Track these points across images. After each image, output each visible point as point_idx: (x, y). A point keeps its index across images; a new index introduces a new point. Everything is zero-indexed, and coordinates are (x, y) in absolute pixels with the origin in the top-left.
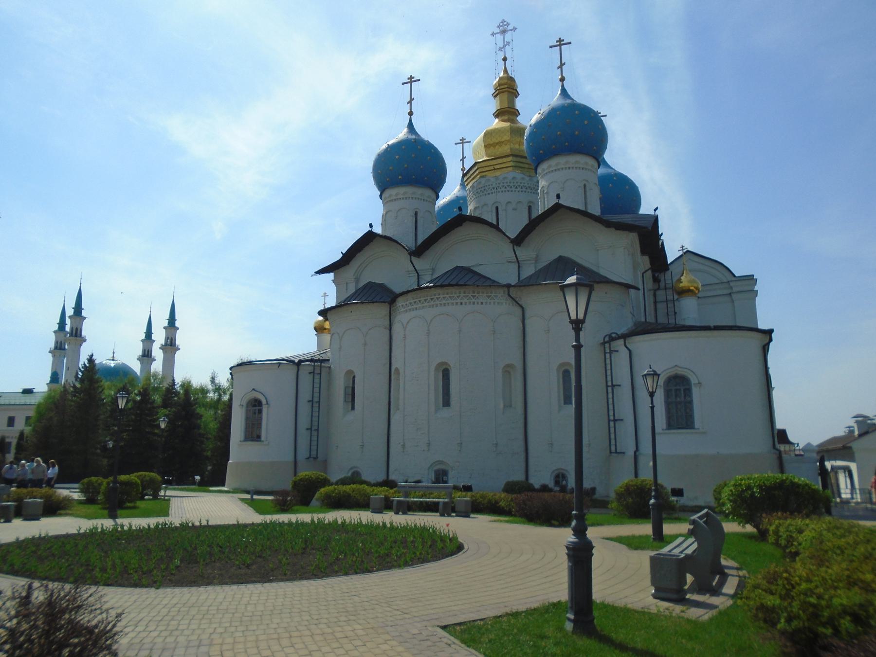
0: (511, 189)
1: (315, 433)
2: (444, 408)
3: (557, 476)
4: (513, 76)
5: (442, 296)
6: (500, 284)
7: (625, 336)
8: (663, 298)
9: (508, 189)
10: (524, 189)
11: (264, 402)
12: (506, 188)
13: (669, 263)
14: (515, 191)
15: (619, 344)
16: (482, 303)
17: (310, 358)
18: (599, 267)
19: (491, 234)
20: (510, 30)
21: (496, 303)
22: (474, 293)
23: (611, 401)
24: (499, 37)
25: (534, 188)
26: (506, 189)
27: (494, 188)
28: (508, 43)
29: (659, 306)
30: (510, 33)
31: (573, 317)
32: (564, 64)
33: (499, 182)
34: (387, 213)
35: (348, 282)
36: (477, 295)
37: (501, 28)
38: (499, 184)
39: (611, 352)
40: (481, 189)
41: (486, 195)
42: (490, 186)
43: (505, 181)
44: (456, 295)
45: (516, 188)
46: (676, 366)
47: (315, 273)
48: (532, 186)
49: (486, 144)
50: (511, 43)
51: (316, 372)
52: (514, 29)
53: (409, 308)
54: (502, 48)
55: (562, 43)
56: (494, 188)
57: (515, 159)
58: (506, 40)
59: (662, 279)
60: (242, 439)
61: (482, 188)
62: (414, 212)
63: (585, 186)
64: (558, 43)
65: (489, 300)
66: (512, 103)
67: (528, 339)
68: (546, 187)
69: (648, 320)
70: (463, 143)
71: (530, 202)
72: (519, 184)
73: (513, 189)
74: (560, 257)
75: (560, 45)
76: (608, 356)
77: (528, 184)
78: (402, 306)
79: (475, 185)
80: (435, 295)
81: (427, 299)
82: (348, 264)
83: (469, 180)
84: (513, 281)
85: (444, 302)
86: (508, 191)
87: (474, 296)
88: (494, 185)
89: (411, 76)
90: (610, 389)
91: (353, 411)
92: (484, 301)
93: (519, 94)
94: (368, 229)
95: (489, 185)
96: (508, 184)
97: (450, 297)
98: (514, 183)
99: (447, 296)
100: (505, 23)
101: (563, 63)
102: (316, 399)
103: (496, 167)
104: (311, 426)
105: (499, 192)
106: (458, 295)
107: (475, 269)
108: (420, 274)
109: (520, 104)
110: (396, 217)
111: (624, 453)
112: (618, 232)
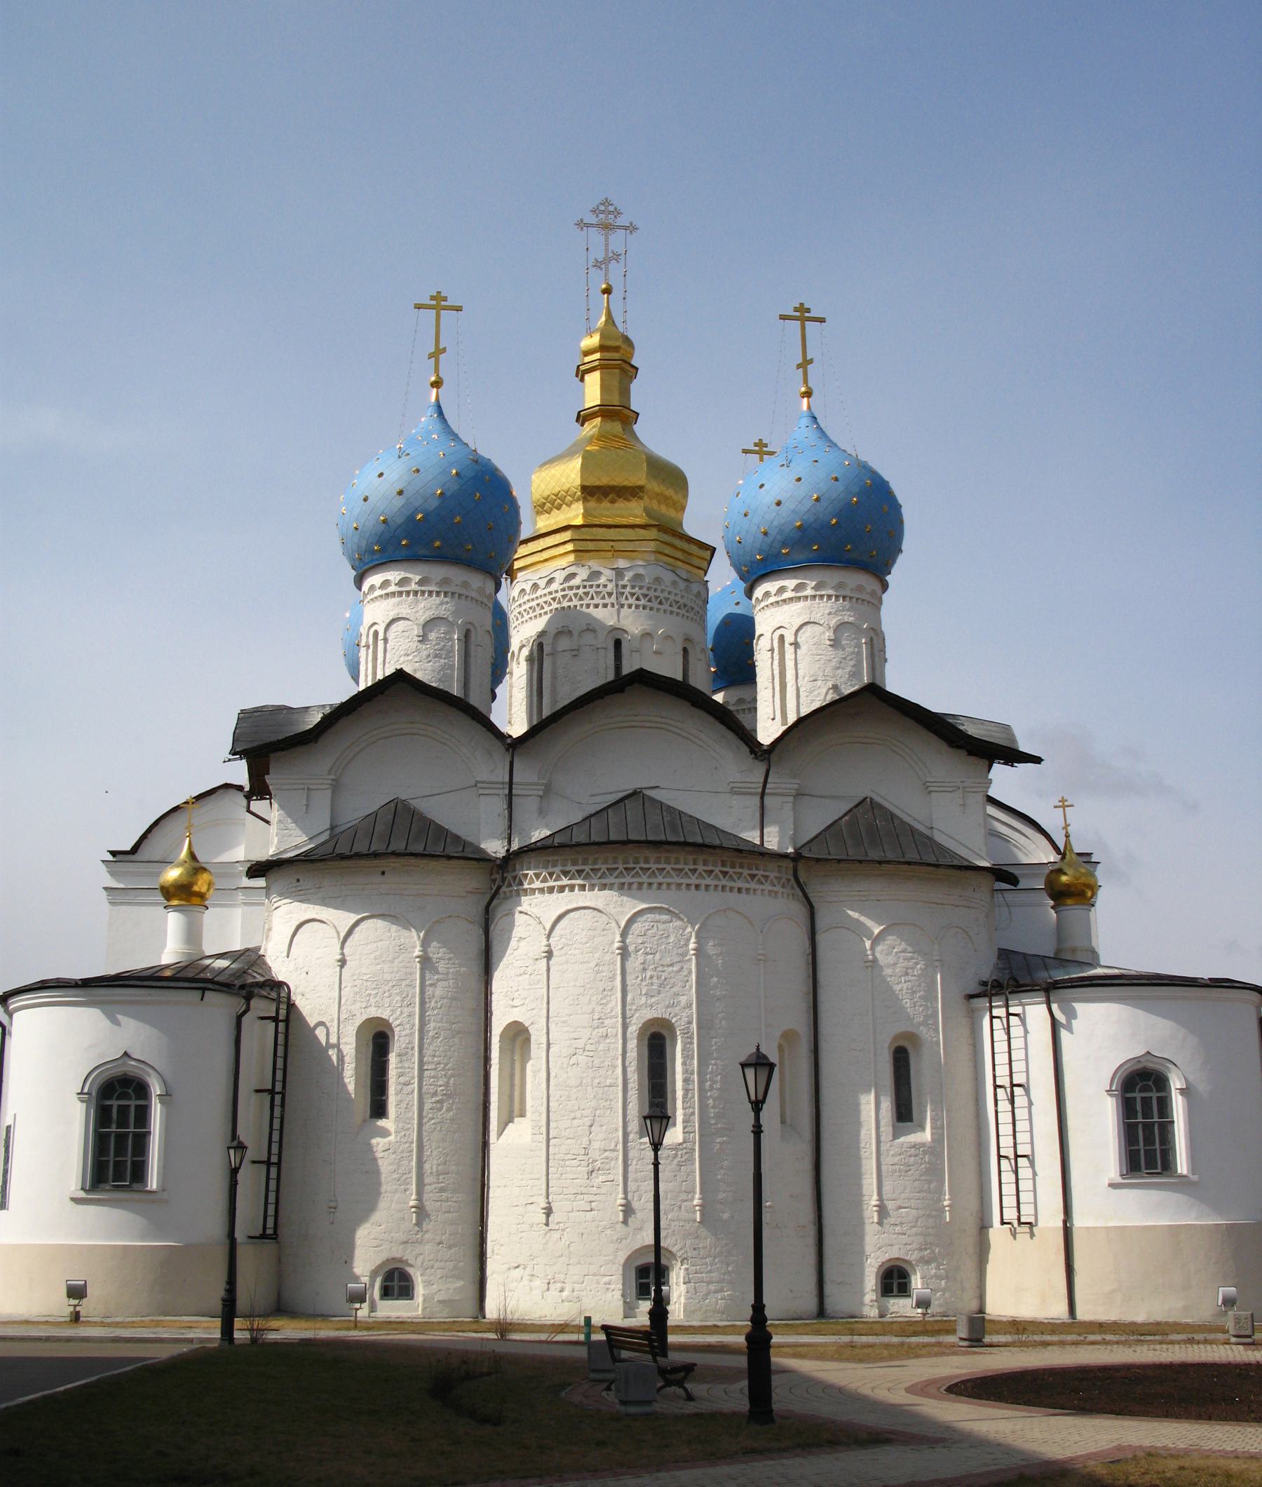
5: (654, 867)
10: (675, 609)
11: (156, 1089)
16: (739, 890)
18: (932, 828)
20: (626, 228)
21: (766, 892)
22: (724, 864)
24: (596, 236)
27: (610, 594)
28: (617, 257)
35: (311, 787)
37: (601, 216)
38: (624, 587)
40: (574, 591)
42: (601, 588)
44: (687, 868)
45: (660, 603)
48: (689, 604)
49: (586, 484)
50: (622, 257)
52: (631, 228)
53: (559, 883)
55: (807, 315)
56: (610, 594)
58: (610, 248)
61: (578, 587)
63: (872, 640)
65: (753, 885)
66: (625, 392)
72: (666, 595)
73: (655, 604)
77: (682, 597)
79: (560, 576)
81: (618, 868)
82: (316, 742)
85: (660, 879)
87: (725, 874)
88: (610, 587)
92: (744, 885)
96: (644, 591)
97: (672, 869)
98: (655, 590)
99: (668, 867)
103: (619, 546)
104: (269, 1158)
106: (692, 867)
110: (423, 639)
112: (972, 758)
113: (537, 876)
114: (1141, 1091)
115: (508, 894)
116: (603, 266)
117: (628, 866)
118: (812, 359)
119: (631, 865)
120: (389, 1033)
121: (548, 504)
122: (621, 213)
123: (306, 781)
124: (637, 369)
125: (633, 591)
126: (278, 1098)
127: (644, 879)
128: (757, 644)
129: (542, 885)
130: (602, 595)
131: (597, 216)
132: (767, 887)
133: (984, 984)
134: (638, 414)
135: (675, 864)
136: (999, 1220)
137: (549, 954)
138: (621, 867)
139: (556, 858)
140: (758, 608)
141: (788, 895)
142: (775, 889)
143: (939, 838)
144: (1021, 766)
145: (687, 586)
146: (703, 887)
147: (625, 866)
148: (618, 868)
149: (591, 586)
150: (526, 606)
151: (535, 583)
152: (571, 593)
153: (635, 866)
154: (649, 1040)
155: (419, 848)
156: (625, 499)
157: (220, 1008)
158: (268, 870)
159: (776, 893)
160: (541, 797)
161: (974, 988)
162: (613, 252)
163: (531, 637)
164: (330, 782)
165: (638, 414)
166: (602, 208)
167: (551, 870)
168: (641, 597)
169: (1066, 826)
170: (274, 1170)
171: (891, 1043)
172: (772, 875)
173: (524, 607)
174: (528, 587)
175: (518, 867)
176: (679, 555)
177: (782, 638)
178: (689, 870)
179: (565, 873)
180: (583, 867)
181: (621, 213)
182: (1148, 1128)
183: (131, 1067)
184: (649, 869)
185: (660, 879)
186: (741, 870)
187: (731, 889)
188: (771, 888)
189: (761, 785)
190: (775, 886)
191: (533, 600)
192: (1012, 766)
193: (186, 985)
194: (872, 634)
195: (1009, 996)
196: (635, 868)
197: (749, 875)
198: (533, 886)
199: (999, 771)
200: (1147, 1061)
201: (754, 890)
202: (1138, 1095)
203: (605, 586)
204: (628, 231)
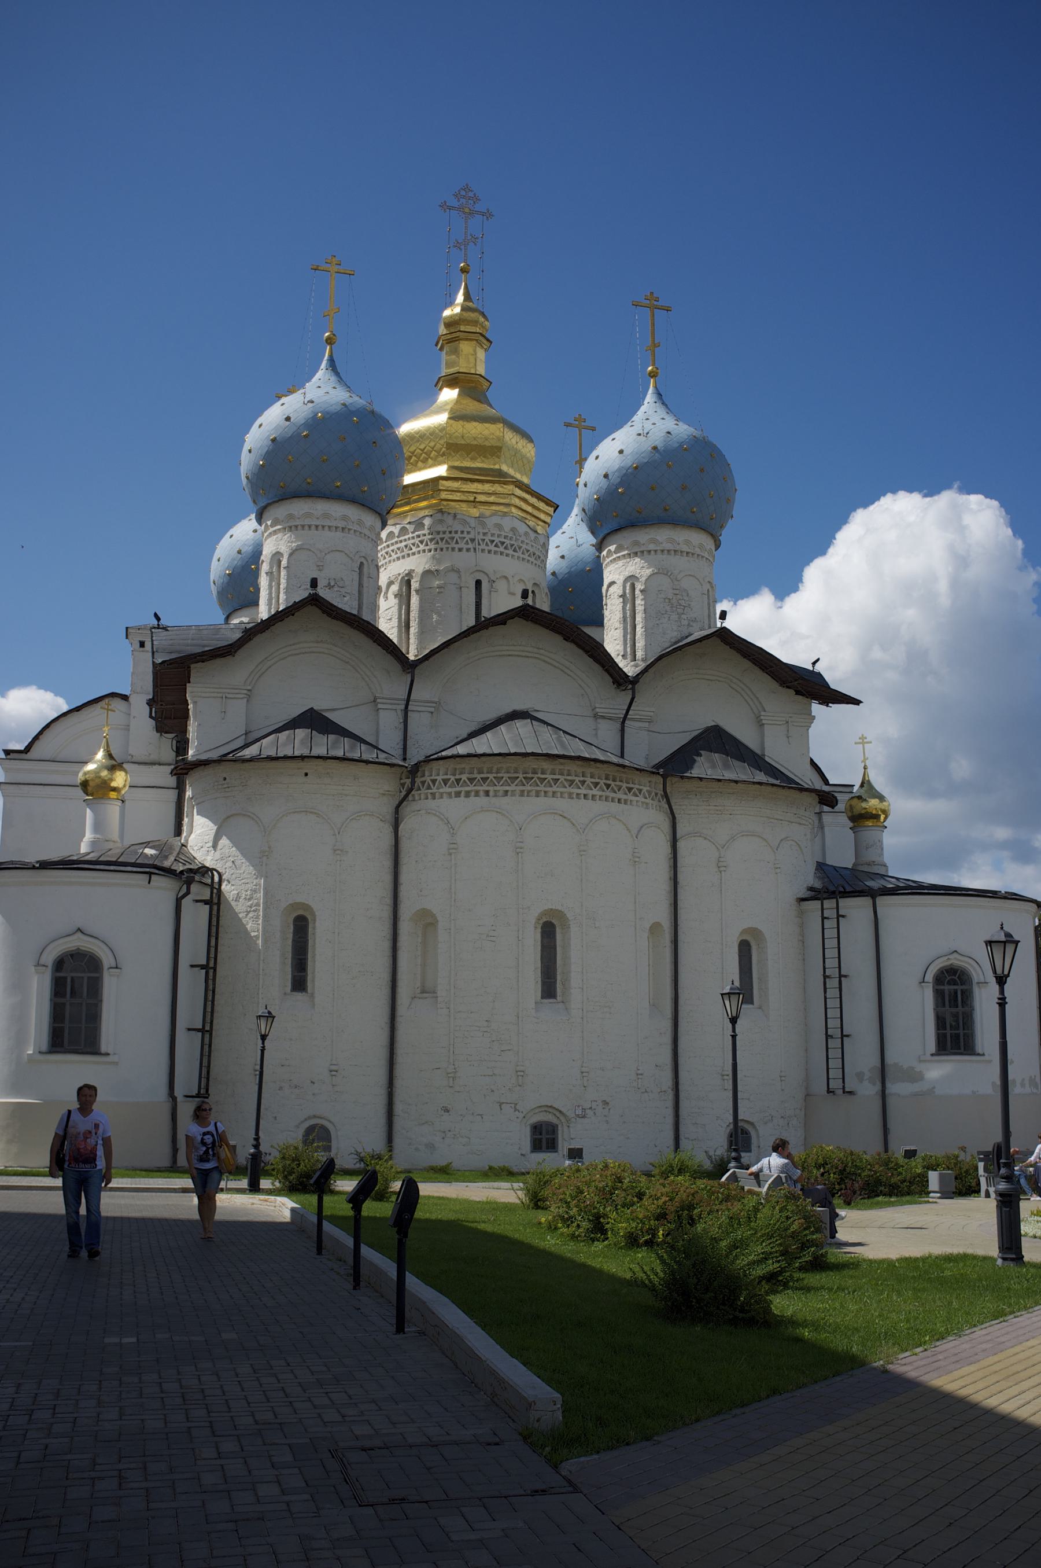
0: (507, 551)
5: (549, 777)
9: (502, 549)
10: (526, 557)
11: (107, 960)
12: (495, 546)
15: (856, 909)
16: (619, 801)
22: (607, 779)
26: (496, 549)
27: (472, 540)
30: (479, 217)
33: (485, 531)
35: (228, 695)
36: (613, 784)
38: (485, 534)
41: (453, 549)
42: (465, 535)
45: (514, 551)
46: (956, 951)
52: (488, 215)
57: (518, 492)
60: (44, 1047)
61: (444, 533)
63: (708, 590)
65: (630, 797)
68: (643, 579)
73: (510, 552)
80: (535, 772)
81: (518, 777)
87: (608, 786)
90: (833, 983)
91: (299, 996)
92: (624, 797)
95: (462, 532)
97: (565, 779)
103: (481, 498)
105: (483, 550)
106: (582, 779)
108: (410, 708)
113: (445, 782)
115: (417, 798)
116: (463, 247)
117: (528, 775)
118: (659, 343)
119: (530, 775)
120: (309, 918)
121: (414, 458)
122: (479, 200)
123: (222, 690)
124: (491, 342)
125: (492, 539)
126: (211, 972)
127: (541, 788)
128: (607, 591)
129: (450, 790)
130: (465, 540)
131: (459, 201)
132: (641, 798)
133: (811, 889)
134: (491, 383)
135: (568, 775)
136: (826, 1089)
138: (521, 776)
139: (463, 766)
140: (608, 560)
144: (836, 708)
145: (536, 537)
147: (525, 775)
148: (518, 777)
149: (456, 532)
150: (395, 547)
151: (404, 527)
152: (438, 537)
153: (533, 776)
154: (542, 928)
155: (340, 754)
156: (484, 457)
157: (164, 890)
158: (192, 769)
159: (647, 804)
160: (432, 713)
161: (803, 893)
162: (471, 235)
163: (399, 574)
164: (245, 692)
165: (491, 383)
166: (463, 193)
167: (457, 777)
168: (499, 544)
169: (865, 760)
170: (207, 1036)
171: (738, 938)
172: (645, 789)
173: (391, 548)
174: (396, 530)
175: (427, 774)
176: (529, 509)
178: (579, 781)
179: (471, 780)
180: (488, 775)
181: (479, 200)
184: (546, 779)
185: (555, 788)
186: (618, 783)
188: (644, 800)
189: (624, 712)
190: (646, 798)
191: (401, 541)
192: (827, 706)
193: (135, 869)
194: (708, 586)
195: (840, 900)
196: (533, 778)
197: (627, 788)
198: (441, 790)
199: (816, 708)
200: (955, 959)
203: (468, 533)
204: (485, 217)
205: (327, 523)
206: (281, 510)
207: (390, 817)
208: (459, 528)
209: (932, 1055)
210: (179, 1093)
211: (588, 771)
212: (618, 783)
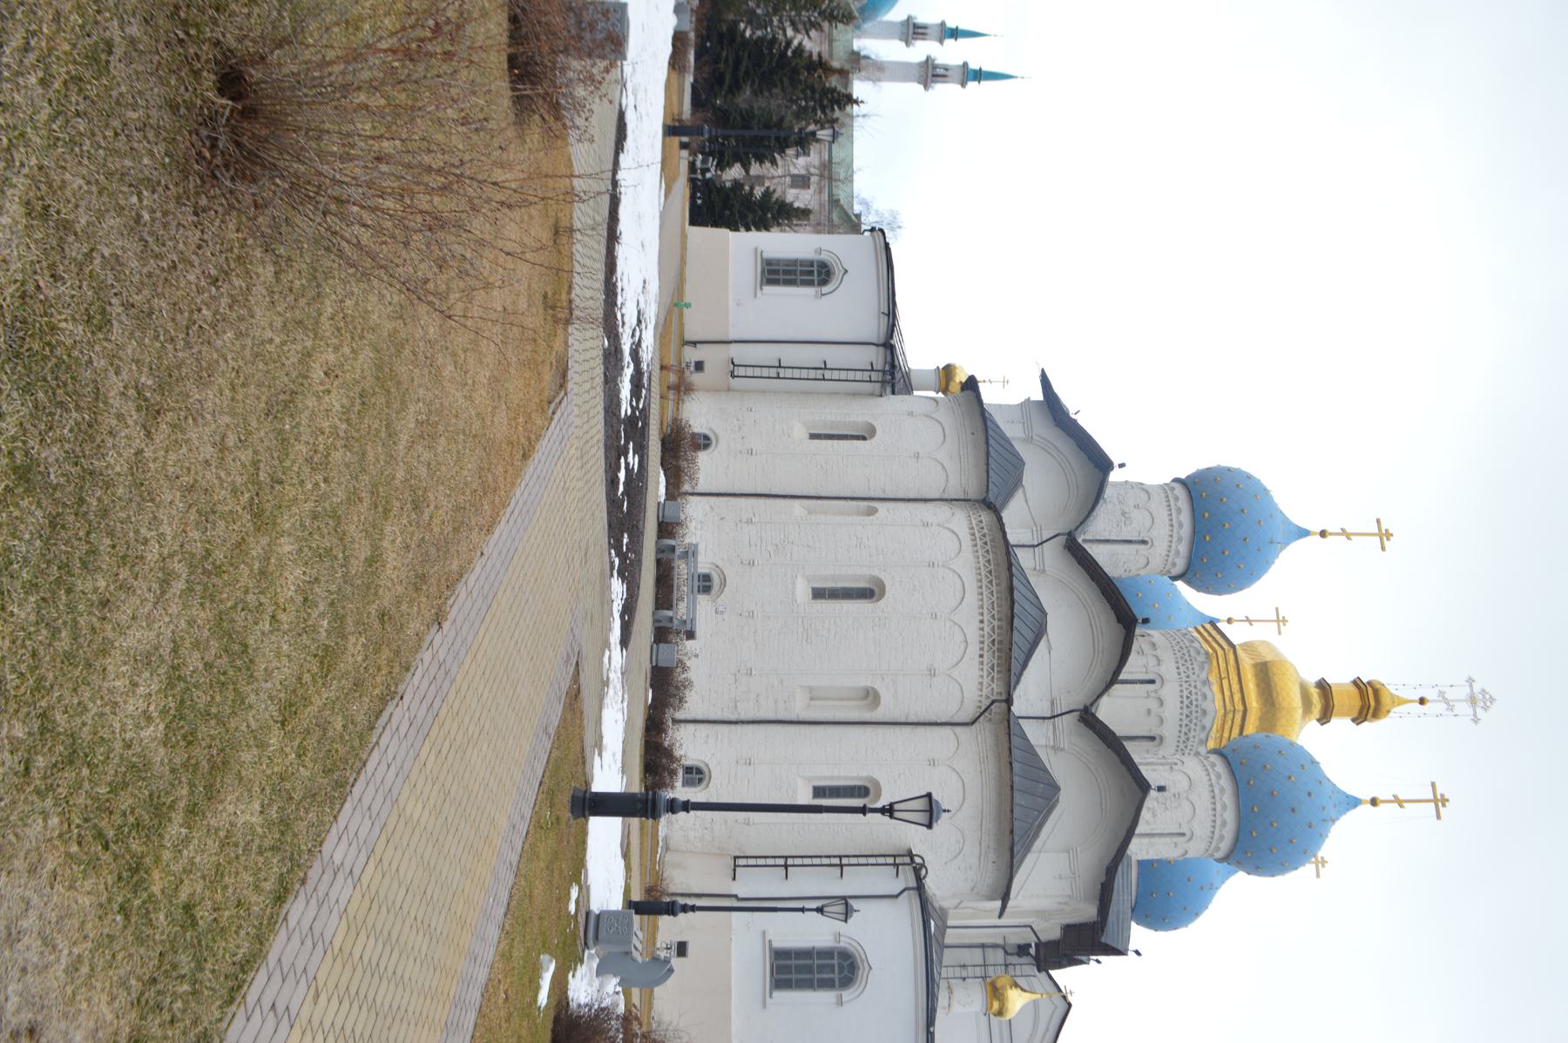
1: (773, 372)
2: (810, 590)
3: (699, 771)
4: (1391, 714)
5: (994, 588)
6: (1015, 688)
7: (920, 888)
8: (990, 960)
10: (1184, 729)
11: (825, 289)
12: (1188, 697)
13: (1051, 972)
14: (1182, 714)
16: (981, 656)
17: (896, 363)
19: (1099, 673)
20: (1475, 715)
23: (817, 861)
25: (1186, 747)
27: (1188, 677)
29: (979, 951)
30: (1471, 711)
31: (896, 807)
32: (1401, 806)
34: (1147, 492)
36: (995, 648)
38: (1195, 687)
39: (896, 865)
41: (1177, 662)
43: (1200, 698)
44: (995, 612)
45: (1187, 716)
46: (871, 968)
47: (1043, 370)
48: (1190, 743)
51: (873, 373)
52: (1476, 720)
54: (1444, 698)
55: (1440, 804)
56: (1188, 677)
58: (1456, 704)
59: (1024, 960)
62: (1146, 539)
63: (1183, 834)
64: (1439, 797)
65: (986, 667)
67: (921, 730)
69: (948, 931)
70: (1278, 621)
71: (1161, 739)
72: (1194, 721)
73: (1185, 711)
74: (1056, 788)
75: (1435, 801)
76: (890, 860)
77: (1194, 737)
78: (981, 522)
79: (1196, 644)
82: (1057, 426)
83: (1206, 634)
84: (1017, 709)
85: (985, 593)
86: (1182, 702)
89: (1392, 535)
90: (836, 861)
91: (808, 436)
92: (985, 659)
93: (1358, 724)
94: (1116, 461)
96: (1194, 703)
98: (1197, 712)
99: (994, 599)
100: (1488, 704)
101: (1404, 804)
102: (828, 374)
103: (1225, 682)
105: (1181, 686)
106: (996, 616)
107: (1042, 645)
108: (1036, 549)
109: (1341, 725)
111: (734, 879)
112: (1099, 887)
114: (839, 964)
127: (985, 582)
132: (986, 680)
137: (926, 525)
141: (980, 701)
142: (984, 689)
143: (1030, 859)
146: (982, 625)
152: (1185, 651)
159: (981, 690)
170: (773, 372)
177: (1176, 764)
179: (984, 536)
182: (809, 969)
183: (838, 273)
187: (982, 649)
194: (1188, 834)
200: (864, 969)
201: (982, 669)
202: (835, 962)
205: (1175, 539)
206: (1180, 491)
207: (946, 496)
208: (1196, 667)
209: (770, 941)
210: (735, 351)
211: (1004, 624)
212: (996, 654)
